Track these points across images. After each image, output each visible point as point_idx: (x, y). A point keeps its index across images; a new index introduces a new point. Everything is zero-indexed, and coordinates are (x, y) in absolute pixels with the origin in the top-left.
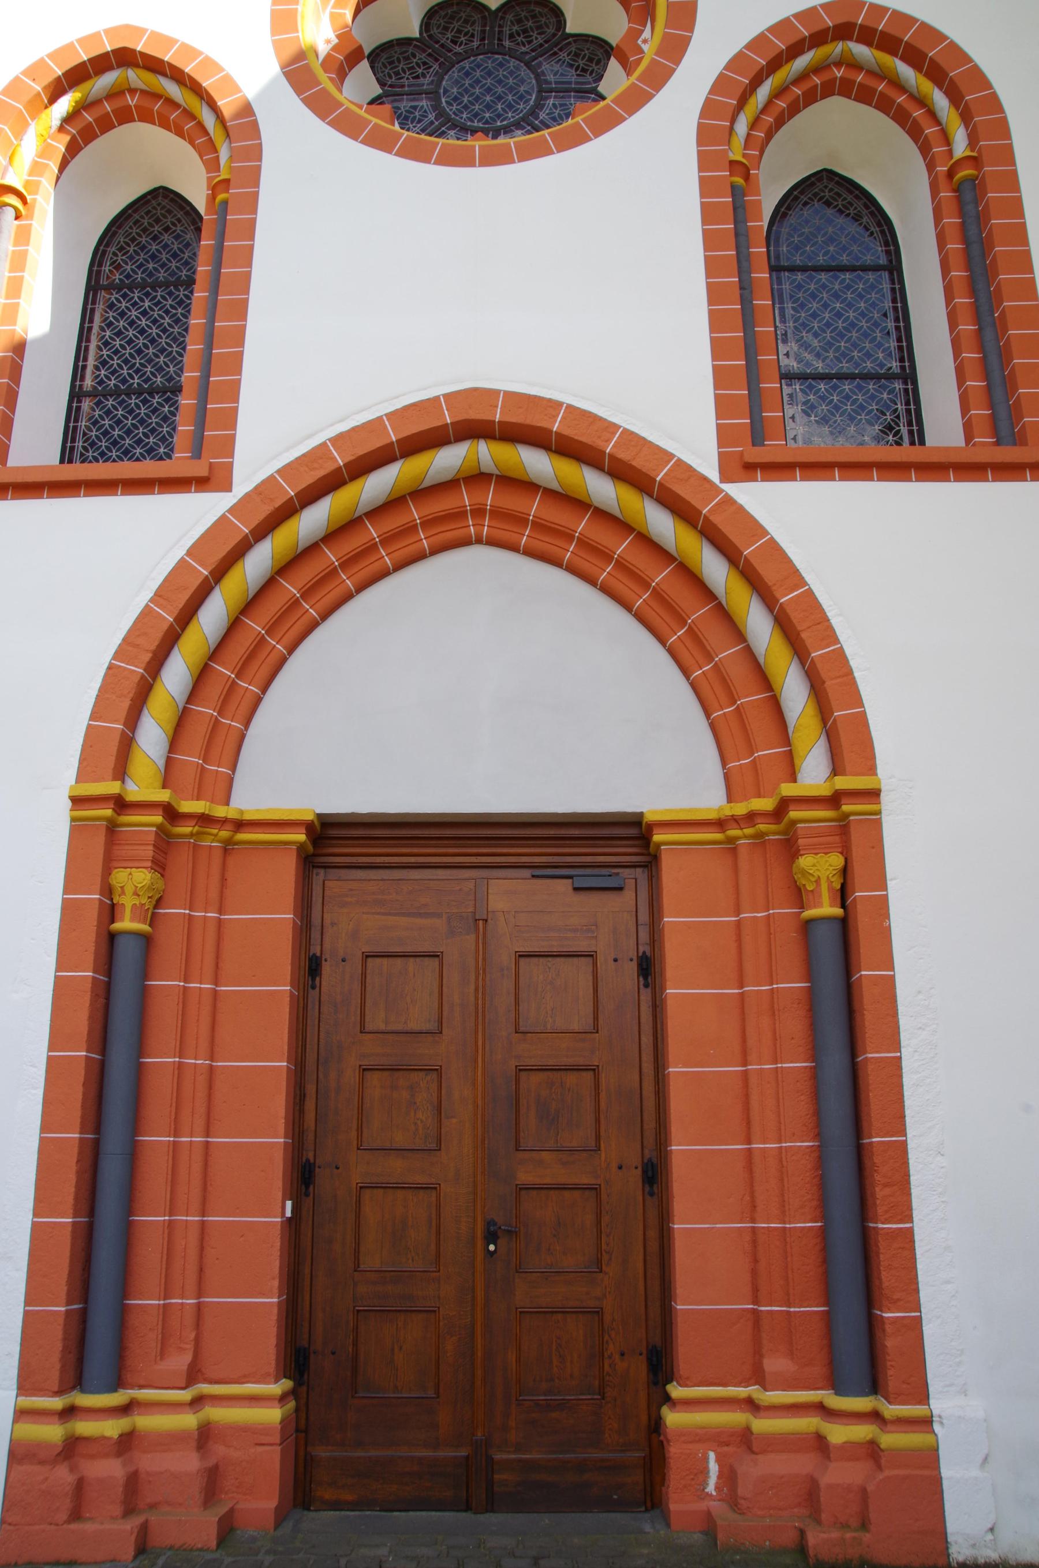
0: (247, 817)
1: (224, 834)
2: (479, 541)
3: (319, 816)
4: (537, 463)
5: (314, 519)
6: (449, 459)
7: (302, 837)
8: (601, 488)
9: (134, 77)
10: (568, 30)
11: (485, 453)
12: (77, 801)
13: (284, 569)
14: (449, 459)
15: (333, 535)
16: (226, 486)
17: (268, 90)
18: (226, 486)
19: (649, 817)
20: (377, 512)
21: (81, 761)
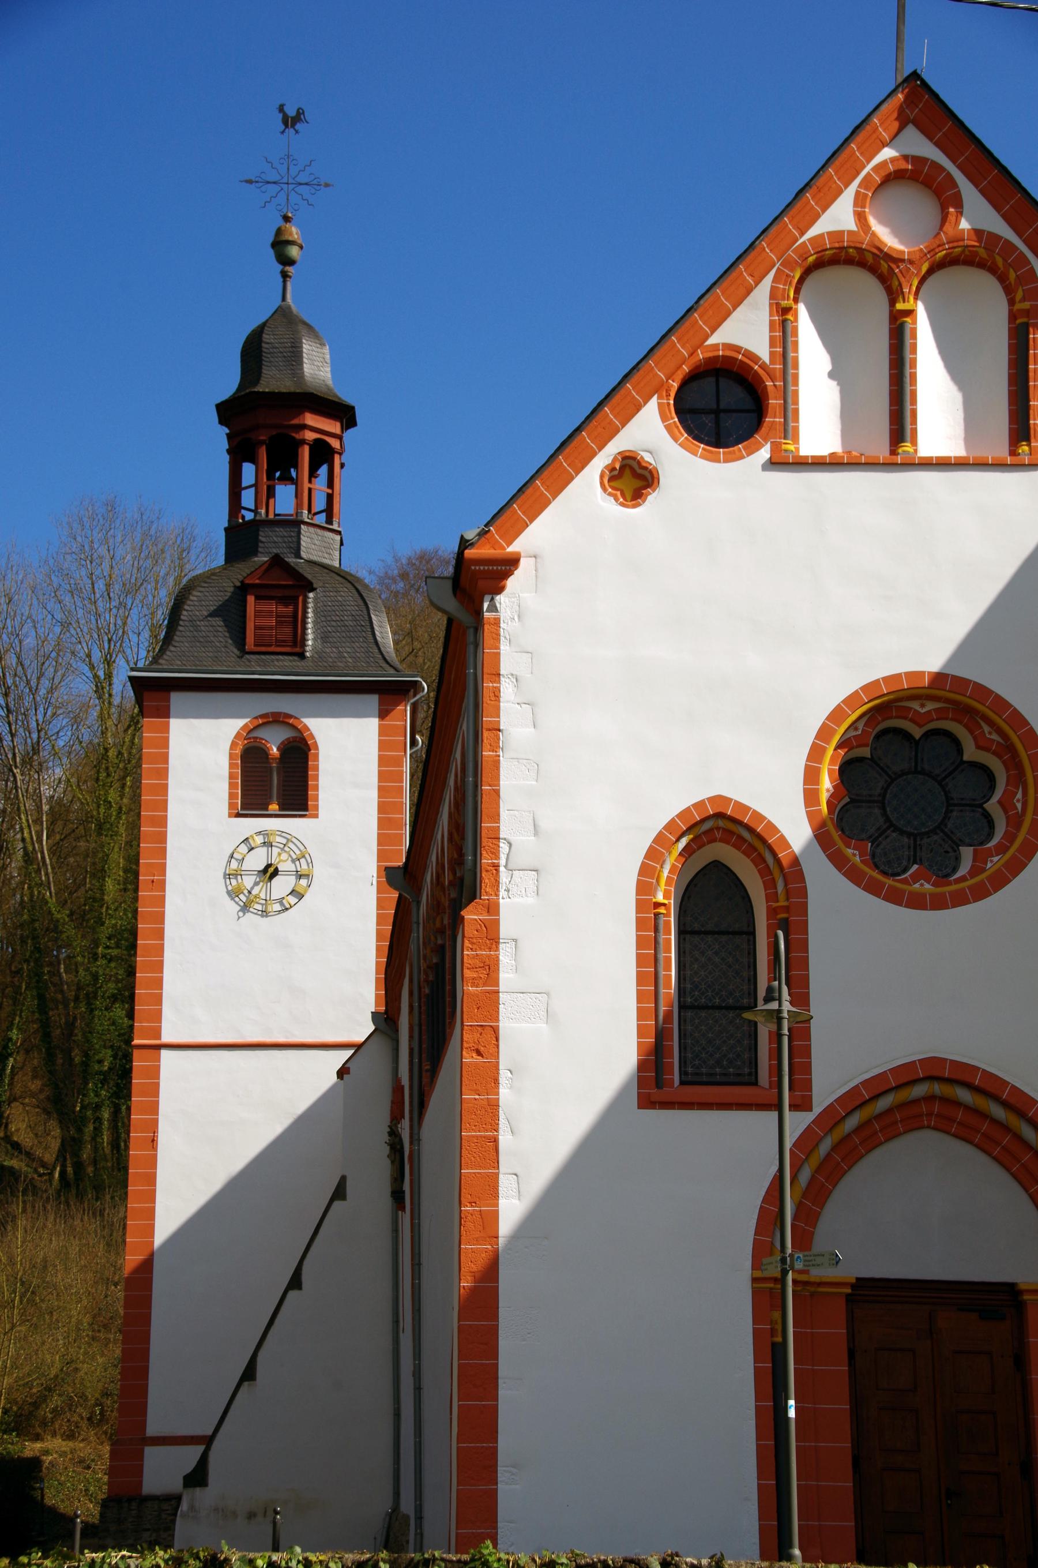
0: (824, 1280)
1: (813, 1289)
2: (929, 1127)
3: (858, 1279)
4: (964, 1095)
5: (852, 1122)
6: (920, 1090)
7: (849, 1291)
8: (998, 1112)
9: (721, 823)
10: (965, 758)
11: (937, 1088)
12: (754, 1280)
13: (835, 1148)
14: (920, 1090)
15: (858, 1130)
16: (810, 1109)
17: (807, 848)
18: (810, 1109)
19: (1023, 1287)
20: (879, 1117)
21: (753, 1257)
